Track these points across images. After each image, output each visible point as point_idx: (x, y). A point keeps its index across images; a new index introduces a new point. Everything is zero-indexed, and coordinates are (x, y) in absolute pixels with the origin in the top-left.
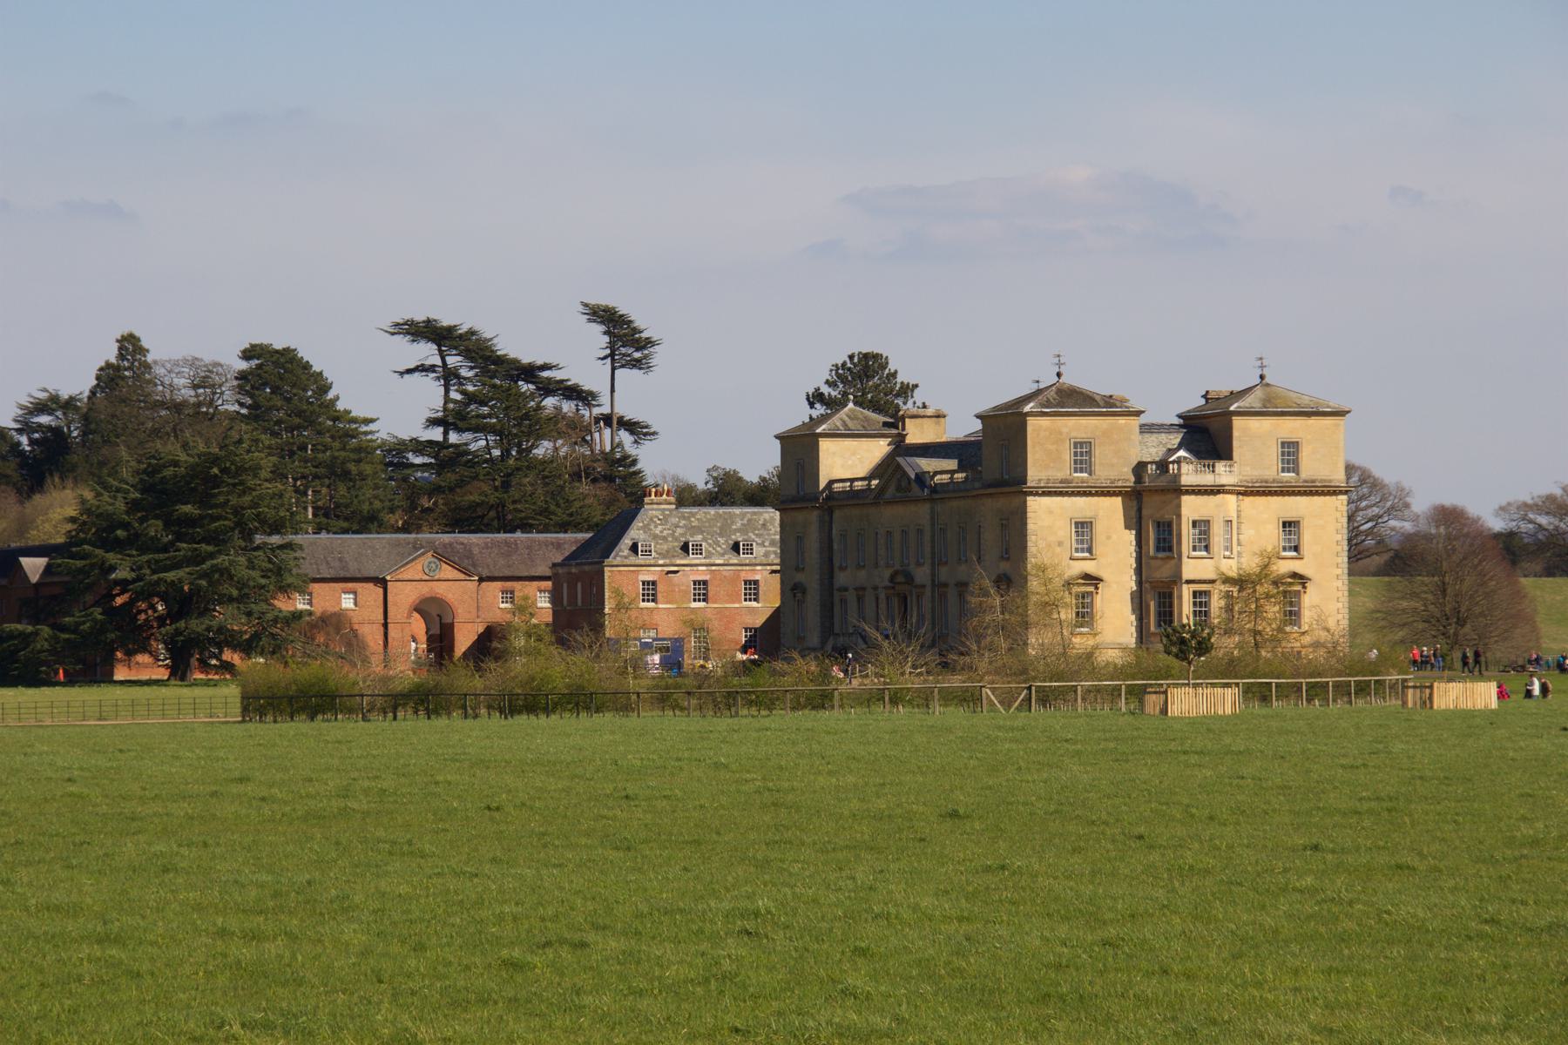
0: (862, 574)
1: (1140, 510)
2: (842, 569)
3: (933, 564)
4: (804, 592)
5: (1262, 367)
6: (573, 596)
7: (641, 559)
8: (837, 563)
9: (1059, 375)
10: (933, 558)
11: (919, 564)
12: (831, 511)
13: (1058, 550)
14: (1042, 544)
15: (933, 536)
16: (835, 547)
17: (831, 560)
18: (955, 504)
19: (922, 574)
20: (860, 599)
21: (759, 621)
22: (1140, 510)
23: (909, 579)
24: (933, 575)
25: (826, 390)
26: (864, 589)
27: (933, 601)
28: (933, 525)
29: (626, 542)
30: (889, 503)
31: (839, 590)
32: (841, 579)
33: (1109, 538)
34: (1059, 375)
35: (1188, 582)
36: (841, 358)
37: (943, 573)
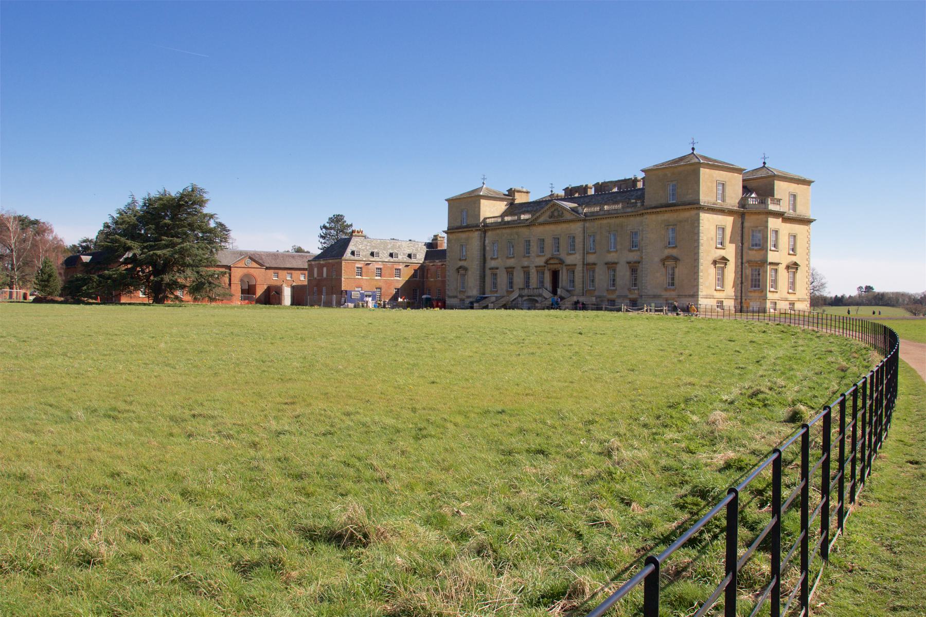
1: (742, 223)
5: (764, 158)
6: (320, 273)
7: (356, 258)
8: (488, 257)
9: (693, 149)
12: (485, 232)
14: (705, 238)
16: (488, 248)
17: (484, 255)
18: (605, 222)
21: (399, 286)
22: (742, 223)
23: (562, 262)
25: (327, 225)
29: (349, 251)
30: (540, 224)
32: (491, 264)
34: (693, 149)
35: (771, 264)
36: (331, 216)
37: (591, 259)
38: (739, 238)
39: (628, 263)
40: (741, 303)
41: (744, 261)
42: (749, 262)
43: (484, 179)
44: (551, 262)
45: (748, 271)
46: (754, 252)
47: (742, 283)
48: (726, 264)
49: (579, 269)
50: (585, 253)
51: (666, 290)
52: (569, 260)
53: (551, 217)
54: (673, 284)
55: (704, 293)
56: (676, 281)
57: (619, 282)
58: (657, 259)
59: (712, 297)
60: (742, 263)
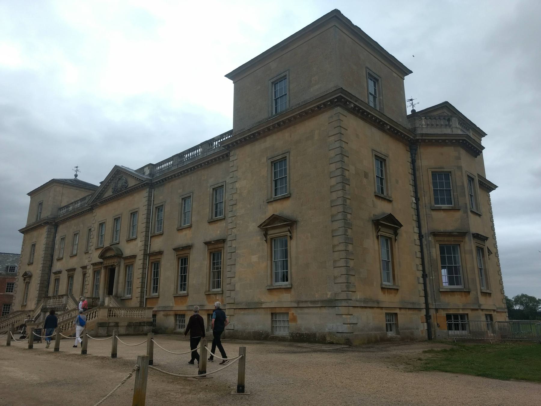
0: (75, 259)
2: (59, 259)
3: (147, 236)
4: (30, 277)
8: (56, 257)
10: (147, 232)
11: (129, 240)
13: (365, 181)
15: (148, 214)
16: (57, 247)
17: (52, 256)
19: (133, 248)
20: (71, 278)
22: (413, 162)
23: (119, 255)
24: (146, 245)
26: (74, 270)
27: (144, 268)
28: (149, 205)
31: (55, 273)
32: (57, 266)
33: (397, 182)
37: (157, 245)
38: (411, 188)
39: (207, 243)
40: (428, 317)
41: (424, 231)
42: (435, 234)
43: (77, 171)
44: (108, 254)
45: (435, 252)
46: (442, 214)
47: (424, 276)
48: (396, 234)
49: (139, 263)
50: (149, 237)
51: (271, 290)
52: (128, 250)
53: (115, 190)
54: (285, 278)
55: (359, 296)
56: (293, 270)
57: (193, 279)
58: (253, 227)
59: (369, 304)
60: (421, 236)
